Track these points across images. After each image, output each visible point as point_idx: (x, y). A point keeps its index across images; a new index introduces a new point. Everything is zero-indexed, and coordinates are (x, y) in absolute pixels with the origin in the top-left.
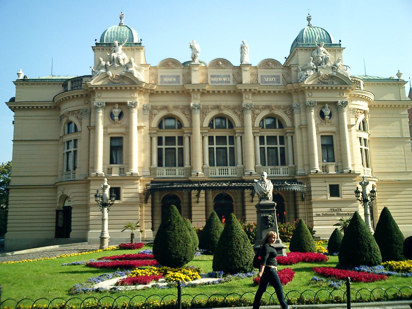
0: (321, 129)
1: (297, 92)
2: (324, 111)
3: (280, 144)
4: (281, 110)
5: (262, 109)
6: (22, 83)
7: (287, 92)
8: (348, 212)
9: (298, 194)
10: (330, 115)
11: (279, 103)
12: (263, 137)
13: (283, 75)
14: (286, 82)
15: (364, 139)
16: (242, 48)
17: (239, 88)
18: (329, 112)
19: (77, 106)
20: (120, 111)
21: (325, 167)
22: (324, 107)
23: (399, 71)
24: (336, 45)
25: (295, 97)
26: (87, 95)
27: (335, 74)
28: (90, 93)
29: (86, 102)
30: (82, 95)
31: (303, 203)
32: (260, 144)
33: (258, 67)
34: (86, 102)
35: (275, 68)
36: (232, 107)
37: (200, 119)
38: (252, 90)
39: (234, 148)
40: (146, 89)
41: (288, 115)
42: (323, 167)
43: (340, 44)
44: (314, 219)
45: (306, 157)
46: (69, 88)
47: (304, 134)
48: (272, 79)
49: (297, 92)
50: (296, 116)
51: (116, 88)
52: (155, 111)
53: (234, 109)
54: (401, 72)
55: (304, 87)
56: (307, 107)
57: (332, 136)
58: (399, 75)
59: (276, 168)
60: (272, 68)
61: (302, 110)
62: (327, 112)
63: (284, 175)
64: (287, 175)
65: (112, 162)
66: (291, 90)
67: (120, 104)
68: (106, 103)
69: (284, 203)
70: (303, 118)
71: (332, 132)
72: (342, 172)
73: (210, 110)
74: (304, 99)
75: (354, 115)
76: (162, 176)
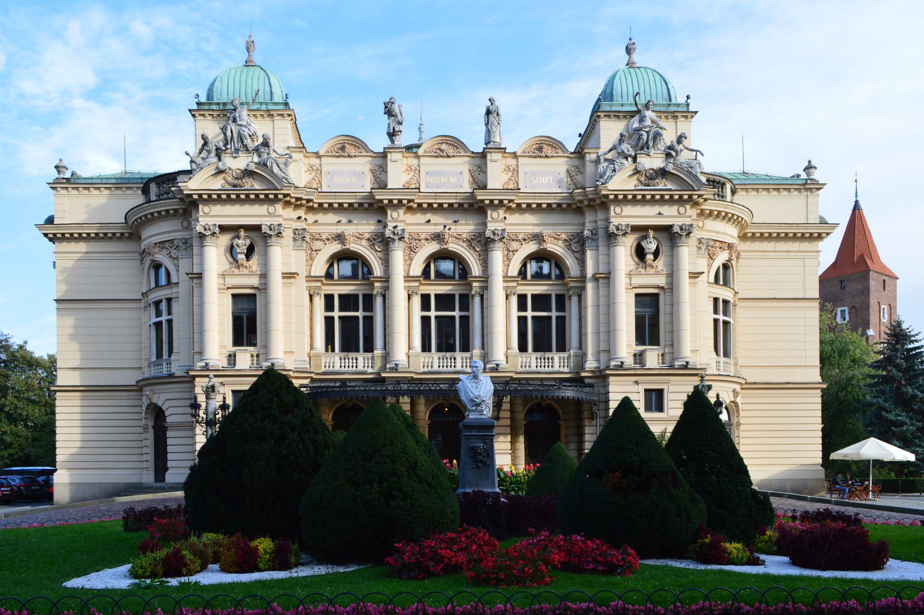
0: (636, 281)
1: (593, 206)
2: (644, 244)
3: (557, 310)
6: (66, 181)
7: (574, 206)
9: (585, 407)
10: (656, 254)
14: (575, 184)
17: (479, 198)
19: (168, 232)
22: (645, 237)
23: (809, 162)
25: (589, 218)
26: (185, 210)
28: (189, 206)
29: (185, 224)
30: (176, 210)
34: (185, 224)
36: (464, 236)
39: (468, 317)
40: (297, 199)
41: (573, 252)
46: (153, 198)
47: (602, 291)
49: (593, 206)
50: (589, 254)
51: (238, 196)
52: (318, 245)
54: (813, 163)
56: (611, 237)
58: (809, 168)
61: (602, 242)
62: (651, 246)
66: (581, 201)
71: (658, 287)
72: (672, 367)
73: (423, 241)
74: (607, 220)
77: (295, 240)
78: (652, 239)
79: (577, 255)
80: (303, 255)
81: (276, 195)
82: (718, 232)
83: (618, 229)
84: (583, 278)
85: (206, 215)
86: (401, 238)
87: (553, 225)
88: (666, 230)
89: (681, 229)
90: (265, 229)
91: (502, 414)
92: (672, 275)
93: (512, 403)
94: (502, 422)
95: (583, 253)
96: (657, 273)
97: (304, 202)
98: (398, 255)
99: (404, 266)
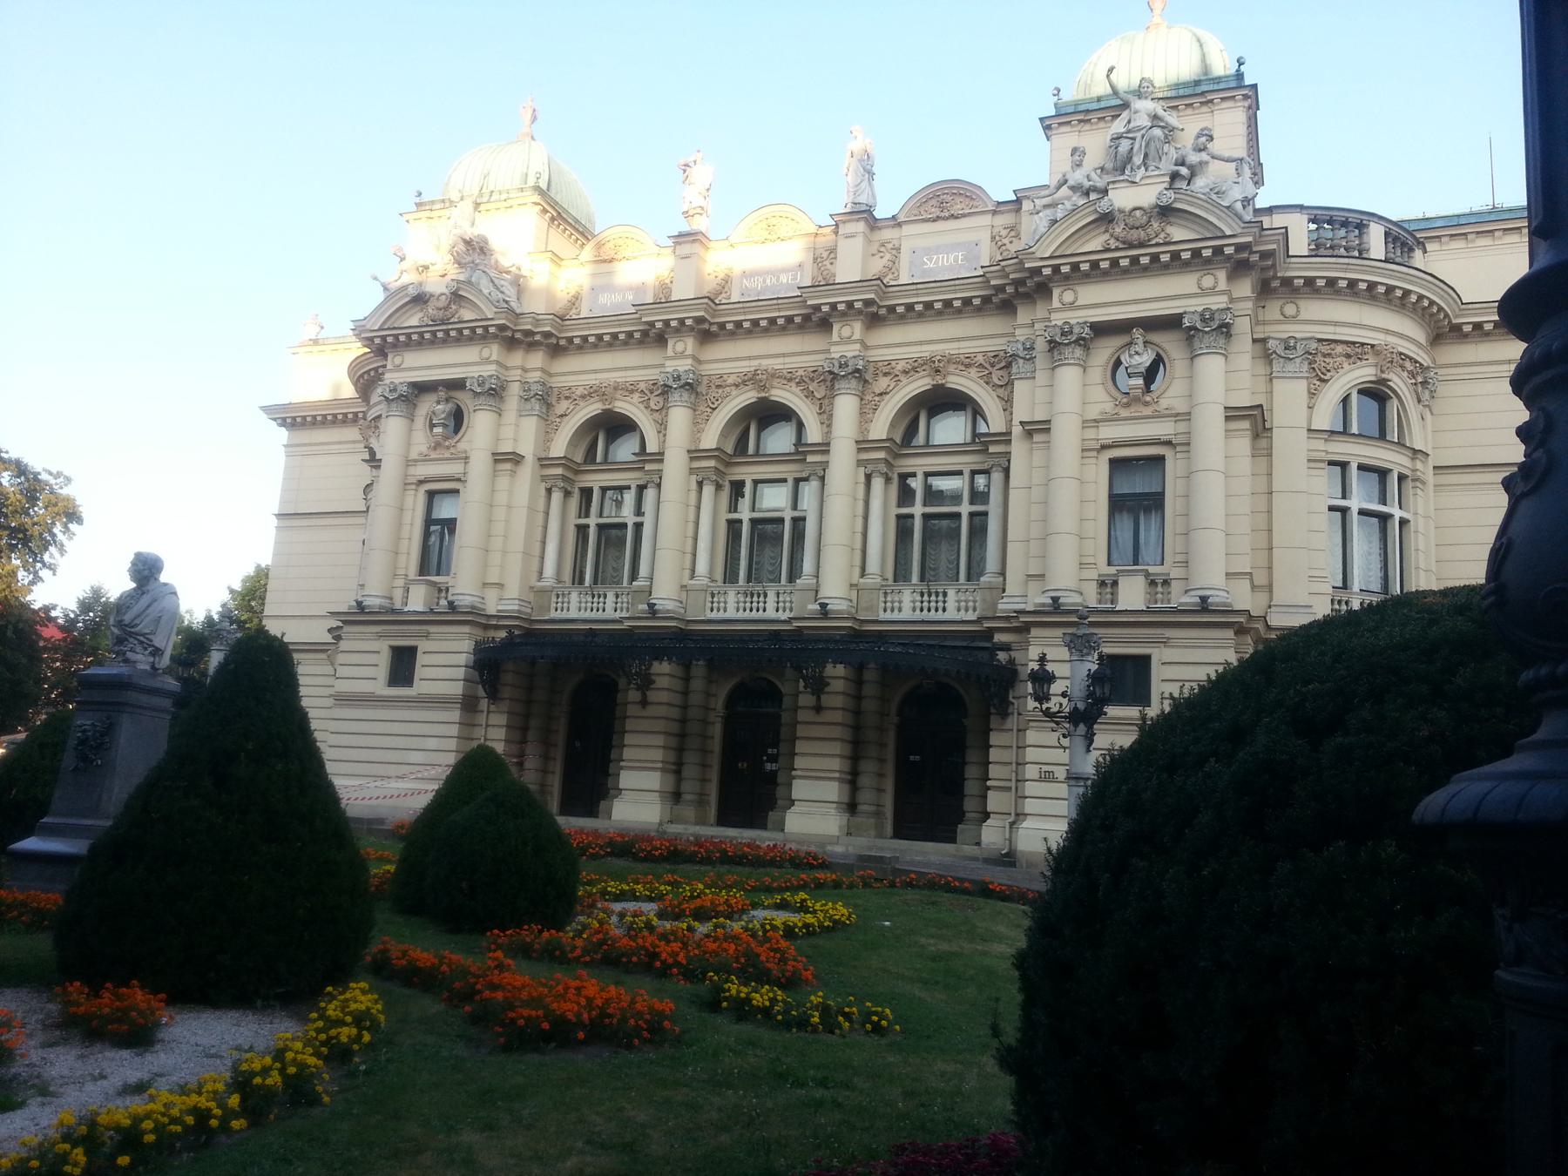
0: (1109, 433)
4: (973, 372)
13: (993, 238)
18: (1146, 359)
20: (449, 407)
21: (1115, 583)
24: (1218, 80)
25: (1023, 315)
32: (899, 506)
33: (901, 218)
35: (964, 216)
36: (801, 372)
37: (696, 424)
38: (858, 305)
42: (1102, 584)
43: (1239, 76)
44: (1030, 788)
48: (952, 258)
50: (1020, 388)
52: (563, 406)
53: (801, 382)
55: (1037, 271)
57: (1160, 459)
60: (953, 217)
61: (1041, 361)
63: (962, 616)
64: (971, 616)
65: (424, 569)
70: (1041, 395)
75: (1305, 367)
76: (564, 615)
78: (1139, 347)
81: (486, 328)
82: (1336, 324)
84: (1005, 438)
85: (398, 368)
86: (690, 387)
88: (1171, 323)
89: (1203, 320)
91: (826, 700)
94: (827, 716)
95: (1009, 384)
96: (1157, 416)
97: (538, 338)
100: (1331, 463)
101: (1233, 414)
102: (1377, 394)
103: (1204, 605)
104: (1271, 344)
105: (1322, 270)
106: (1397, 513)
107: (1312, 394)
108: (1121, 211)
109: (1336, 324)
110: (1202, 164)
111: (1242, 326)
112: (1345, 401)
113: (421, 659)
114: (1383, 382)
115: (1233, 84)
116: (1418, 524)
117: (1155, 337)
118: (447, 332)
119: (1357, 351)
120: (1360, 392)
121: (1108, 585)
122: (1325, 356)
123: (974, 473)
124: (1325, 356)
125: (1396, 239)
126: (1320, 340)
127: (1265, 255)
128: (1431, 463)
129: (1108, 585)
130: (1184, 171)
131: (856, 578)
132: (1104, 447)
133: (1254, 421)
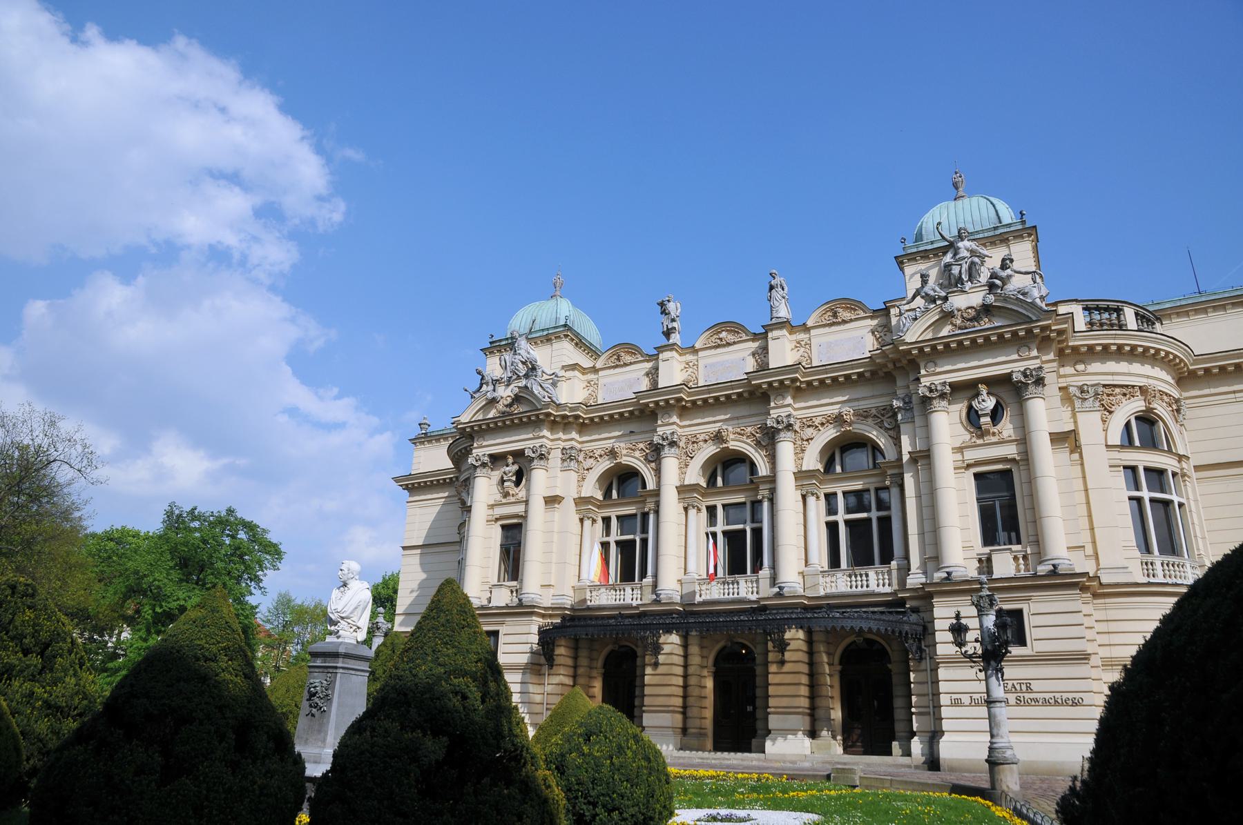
0: (971, 455)
1: (902, 367)
4: (870, 420)
5: (822, 424)
8: (1051, 695)
10: (996, 415)
11: (864, 405)
12: (835, 494)
15: (1146, 469)
16: (772, 288)
18: (990, 403)
21: (989, 560)
22: (978, 394)
24: (1009, 225)
25: (900, 383)
27: (991, 299)
31: (923, 665)
41: (887, 429)
42: (980, 561)
43: (1023, 222)
44: (945, 712)
45: (928, 537)
55: (909, 351)
56: (926, 401)
57: (1010, 471)
59: (858, 572)
63: (881, 590)
64: (888, 589)
67: (518, 455)
68: (491, 456)
69: (890, 666)
75: (1098, 404)
77: (563, 460)
79: (891, 433)
80: (574, 476)
81: (537, 416)
82: (1113, 374)
83: (931, 391)
86: (673, 444)
87: (857, 400)
88: (1005, 379)
90: (528, 453)
92: (1024, 440)
93: (810, 642)
94: (787, 668)
96: (1002, 442)
98: (670, 464)
99: (676, 473)
100: (1125, 467)
101: (1058, 439)
102: (1147, 420)
103: (1054, 573)
104: (1071, 389)
105: (1100, 339)
106: (1176, 499)
107: (1104, 421)
108: (959, 310)
109: (1113, 374)
110: (1009, 277)
111: (1050, 378)
112: (1128, 425)
113: (502, 639)
114: (1150, 410)
115: (1020, 227)
116: (1191, 506)
117: (994, 390)
118: (512, 420)
119: (1128, 390)
120: (1137, 418)
121: (986, 564)
122: (1108, 395)
123: (877, 490)
124: (1108, 395)
125: (1143, 317)
126: (1104, 386)
127: (1060, 332)
128: (1192, 462)
129: (986, 564)
130: (998, 282)
131: (802, 568)
132: (969, 466)
133: (1067, 440)
